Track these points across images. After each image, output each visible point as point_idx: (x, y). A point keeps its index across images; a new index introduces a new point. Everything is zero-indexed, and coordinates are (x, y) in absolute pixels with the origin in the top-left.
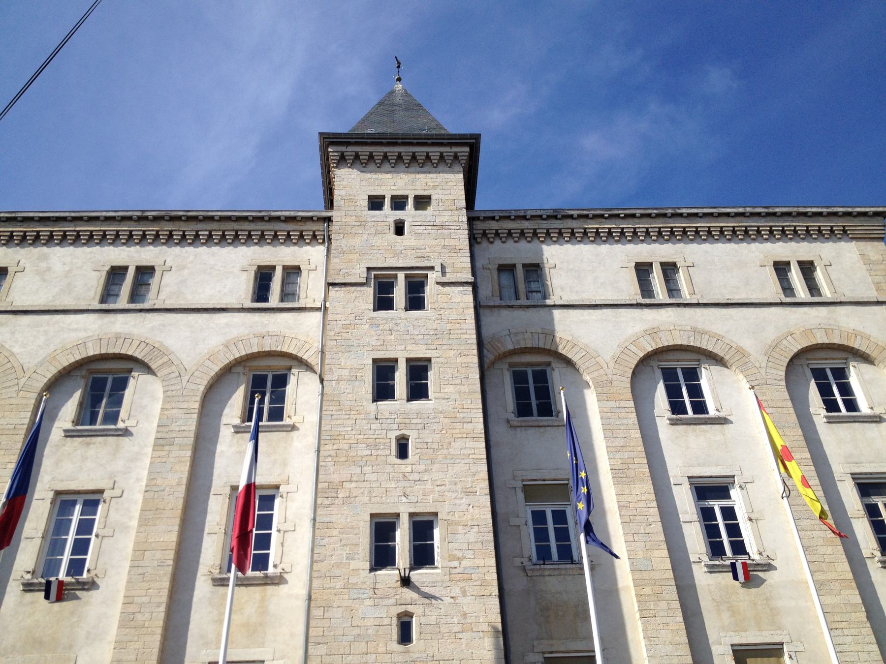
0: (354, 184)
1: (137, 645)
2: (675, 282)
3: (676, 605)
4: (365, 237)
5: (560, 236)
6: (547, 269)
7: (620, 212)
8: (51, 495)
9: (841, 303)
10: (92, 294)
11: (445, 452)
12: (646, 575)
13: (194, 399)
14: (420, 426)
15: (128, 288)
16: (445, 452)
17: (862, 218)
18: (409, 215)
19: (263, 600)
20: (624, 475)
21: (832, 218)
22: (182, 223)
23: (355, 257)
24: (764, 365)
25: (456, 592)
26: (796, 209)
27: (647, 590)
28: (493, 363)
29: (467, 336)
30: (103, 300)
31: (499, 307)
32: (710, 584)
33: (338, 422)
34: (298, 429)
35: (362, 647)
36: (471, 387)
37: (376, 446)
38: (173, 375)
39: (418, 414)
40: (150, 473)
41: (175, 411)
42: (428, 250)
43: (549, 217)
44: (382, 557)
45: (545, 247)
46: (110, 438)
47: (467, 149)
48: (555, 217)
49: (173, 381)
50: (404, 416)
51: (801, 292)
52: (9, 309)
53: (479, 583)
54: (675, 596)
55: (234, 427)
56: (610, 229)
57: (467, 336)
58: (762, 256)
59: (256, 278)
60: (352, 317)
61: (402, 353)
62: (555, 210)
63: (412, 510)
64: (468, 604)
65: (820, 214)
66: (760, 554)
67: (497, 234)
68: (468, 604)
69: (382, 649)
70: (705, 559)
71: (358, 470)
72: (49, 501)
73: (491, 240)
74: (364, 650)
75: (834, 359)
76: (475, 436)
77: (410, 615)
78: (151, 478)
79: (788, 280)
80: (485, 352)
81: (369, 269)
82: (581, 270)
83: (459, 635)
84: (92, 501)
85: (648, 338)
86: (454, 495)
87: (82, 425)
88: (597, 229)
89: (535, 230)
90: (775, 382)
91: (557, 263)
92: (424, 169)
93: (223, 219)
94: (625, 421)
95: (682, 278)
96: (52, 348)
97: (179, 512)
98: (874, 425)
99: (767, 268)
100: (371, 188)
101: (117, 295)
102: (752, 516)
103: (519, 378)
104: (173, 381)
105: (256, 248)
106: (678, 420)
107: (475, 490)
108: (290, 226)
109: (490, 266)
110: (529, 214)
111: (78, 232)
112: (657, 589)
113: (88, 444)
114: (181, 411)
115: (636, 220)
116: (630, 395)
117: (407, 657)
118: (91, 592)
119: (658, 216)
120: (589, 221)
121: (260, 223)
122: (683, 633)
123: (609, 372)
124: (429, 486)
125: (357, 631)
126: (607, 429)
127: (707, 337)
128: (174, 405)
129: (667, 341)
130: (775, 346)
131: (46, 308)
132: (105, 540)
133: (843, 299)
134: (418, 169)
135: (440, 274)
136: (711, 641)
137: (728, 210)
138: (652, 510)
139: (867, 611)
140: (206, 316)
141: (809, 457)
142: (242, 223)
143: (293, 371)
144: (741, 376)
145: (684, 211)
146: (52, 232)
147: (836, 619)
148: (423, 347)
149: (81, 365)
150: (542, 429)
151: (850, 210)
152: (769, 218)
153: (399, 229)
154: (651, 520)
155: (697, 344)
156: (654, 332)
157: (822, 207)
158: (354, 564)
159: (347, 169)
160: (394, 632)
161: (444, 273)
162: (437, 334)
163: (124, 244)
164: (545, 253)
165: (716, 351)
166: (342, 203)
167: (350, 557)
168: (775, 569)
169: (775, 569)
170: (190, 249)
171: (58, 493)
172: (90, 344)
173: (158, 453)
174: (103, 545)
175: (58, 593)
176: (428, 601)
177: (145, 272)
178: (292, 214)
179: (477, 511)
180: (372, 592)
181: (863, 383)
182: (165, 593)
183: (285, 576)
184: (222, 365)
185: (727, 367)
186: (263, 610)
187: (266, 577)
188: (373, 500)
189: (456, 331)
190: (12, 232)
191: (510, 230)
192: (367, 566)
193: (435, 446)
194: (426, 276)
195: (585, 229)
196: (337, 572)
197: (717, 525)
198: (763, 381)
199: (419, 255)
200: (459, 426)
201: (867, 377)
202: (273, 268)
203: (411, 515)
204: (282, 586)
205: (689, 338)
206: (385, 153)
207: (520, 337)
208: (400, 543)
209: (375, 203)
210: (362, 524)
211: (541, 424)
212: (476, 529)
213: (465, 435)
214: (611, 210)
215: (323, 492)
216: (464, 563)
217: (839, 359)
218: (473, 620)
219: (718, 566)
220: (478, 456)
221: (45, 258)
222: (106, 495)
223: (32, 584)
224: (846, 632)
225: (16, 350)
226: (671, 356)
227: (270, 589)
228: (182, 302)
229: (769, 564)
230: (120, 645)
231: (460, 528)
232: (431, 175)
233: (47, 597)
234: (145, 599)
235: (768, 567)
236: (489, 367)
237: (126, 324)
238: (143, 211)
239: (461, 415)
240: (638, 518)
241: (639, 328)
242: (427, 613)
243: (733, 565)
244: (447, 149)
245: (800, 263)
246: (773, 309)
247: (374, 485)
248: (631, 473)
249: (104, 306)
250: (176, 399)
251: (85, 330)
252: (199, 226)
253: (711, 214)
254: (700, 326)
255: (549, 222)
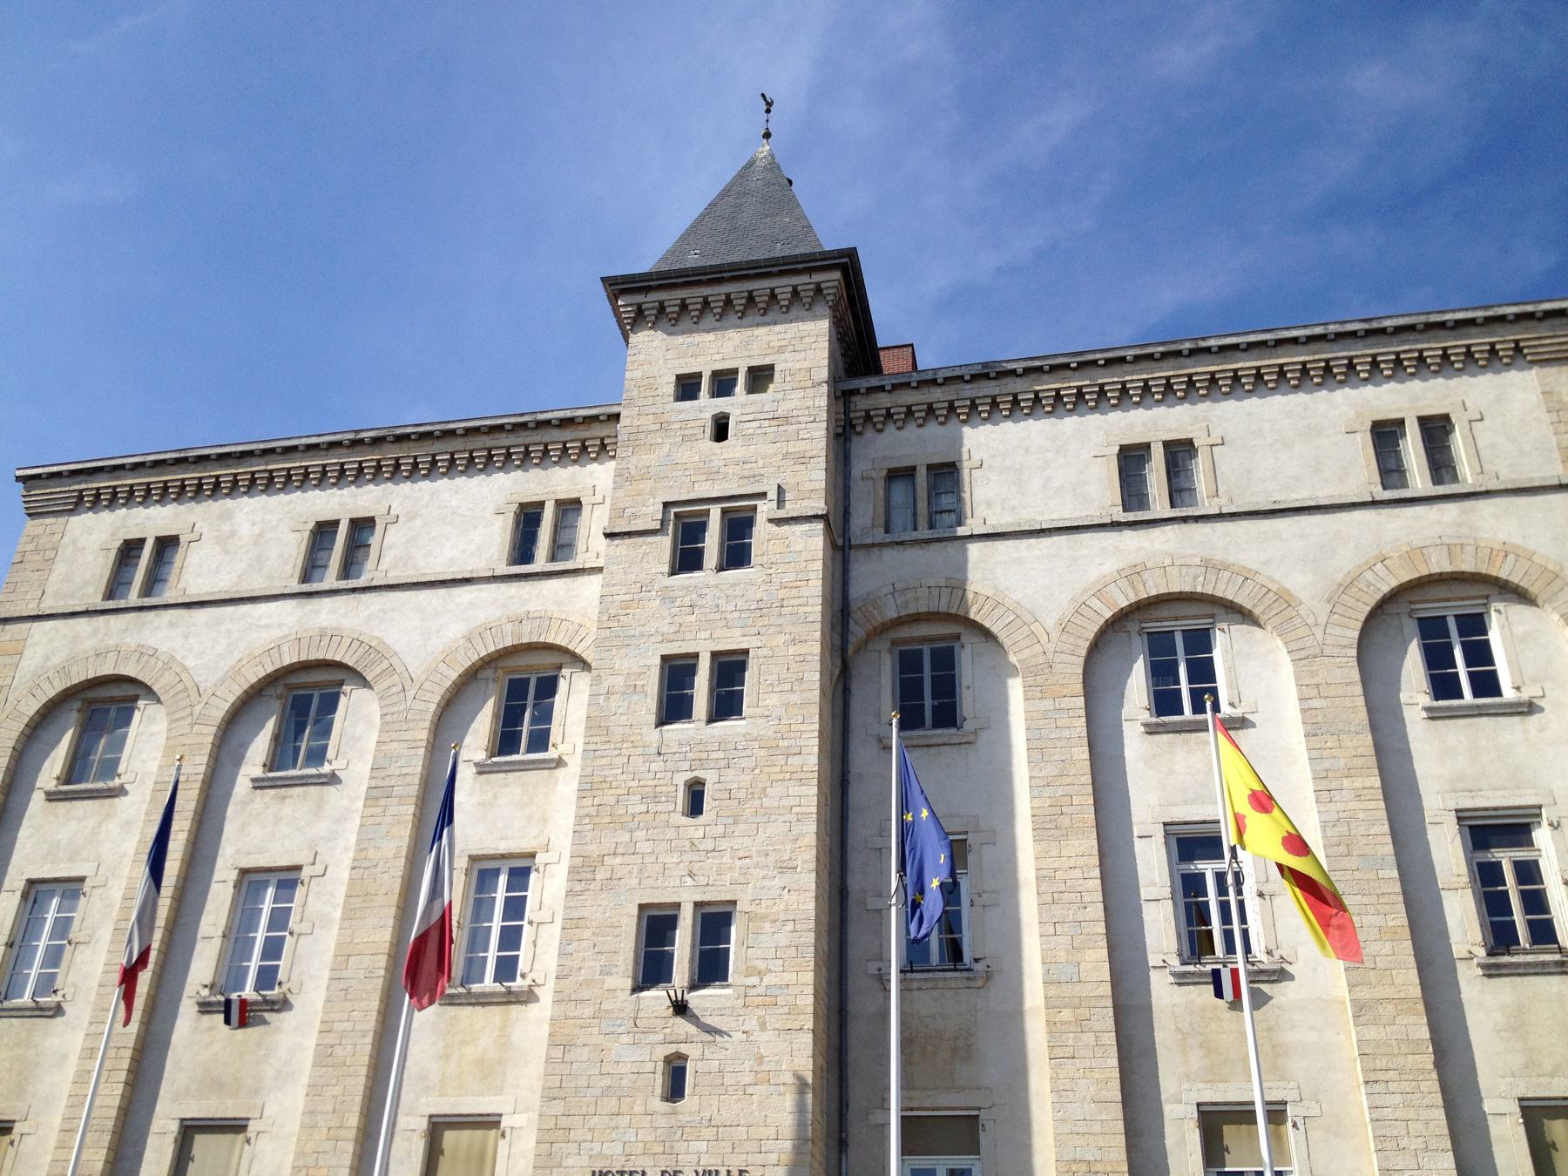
0: (658, 355)
1: (337, 1090)
2: (1189, 474)
3: (1110, 1039)
4: (666, 449)
5: (994, 410)
6: (966, 472)
7: (1098, 356)
8: (234, 875)
9: (1488, 494)
10: (289, 569)
11: (757, 803)
12: (1066, 990)
13: (422, 725)
14: (722, 763)
15: (338, 553)
16: (757, 803)
17: (1557, 322)
18: (738, 404)
19: (504, 1026)
20: (1052, 825)
21: (1497, 327)
22: (411, 444)
23: (647, 485)
24: (1322, 620)
25: (752, 1023)
26: (1423, 319)
27: (1066, 1015)
28: (866, 642)
29: (808, 609)
30: (305, 577)
31: (881, 545)
32: (1173, 1001)
33: (604, 761)
34: (566, 765)
35: (611, 1104)
36: (805, 695)
37: (655, 798)
38: (394, 690)
39: (721, 745)
40: (359, 840)
41: (394, 745)
42: (761, 463)
43: (975, 378)
44: (653, 970)
45: (967, 431)
46: (312, 788)
47: (837, 275)
48: (987, 376)
49: (395, 699)
50: (700, 747)
51: (1419, 478)
52: (180, 601)
53: (786, 1010)
54: (1110, 1023)
55: (477, 765)
56: (1079, 388)
57: (808, 609)
58: (1352, 414)
59: (517, 523)
60: (636, 588)
61: (704, 645)
62: (985, 365)
63: (699, 898)
64: (767, 1042)
65: (1471, 322)
66: (1269, 953)
67: (889, 415)
68: (767, 1042)
69: (638, 1108)
70: (1175, 962)
71: (626, 837)
72: (231, 884)
73: (879, 426)
74: (615, 1110)
75: (1463, 599)
76: (803, 776)
77: (685, 1058)
78: (360, 850)
79: (1398, 455)
80: (852, 626)
81: (666, 505)
82: (1028, 469)
83: (750, 1090)
84: (288, 879)
85: (1123, 583)
86: (763, 873)
87: (278, 769)
88: (1058, 391)
89: (951, 403)
90: (1336, 651)
91: (985, 457)
92: (767, 318)
93: (470, 432)
94: (1066, 733)
95: (1200, 468)
96: (237, 656)
97: (394, 899)
98: (1516, 719)
99: (1358, 435)
100: (681, 361)
101: (325, 567)
102: (1265, 889)
103: (908, 663)
104: (395, 699)
105: (518, 475)
106: (1158, 725)
107: (794, 864)
108: (566, 434)
109: (873, 474)
110: (940, 376)
111: (271, 471)
112: (1084, 1012)
113: (284, 798)
114: (405, 745)
115: (1127, 367)
116: (1080, 686)
117: (673, 1121)
118: (283, 1014)
119: (1165, 355)
120: (1045, 377)
121: (523, 433)
122: (1116, 1084)
123: (1050, 647)
124: (727, 859)
125: (606, 1082)
126: (1036, 749)
127: (1227, 574)
128: (395, 736)
129: (1155, 586)
130: (1348, 586)
131: (228, 596)
132: (302, 938)
133: (1493, 485)
134: (759, 319)
135: (775, 504)
136: (1163, 1097)
137: (1295, 333)
138: (1091, 882)
139: (1435, 1052)
140: (442, 592)
141: (1378, 784)
142: (497, 435)
143: (565, 672)
144: (1280, 643)
145: (1212, 343)
146: (235, 475)
147: (1379, 1065)
148: (738, 632)
149: (276, 679)
150: (933, 751)
151: (1530, 308)
152: (1371, 340)
153: (721, 430)
154: (1087, 899)
155: (1208, 590)
156: (1134, 573)
157: (1475, 309)
158: (611, 982)
159: (647, 332)
160: (658, 1082)
161: (781, 502)
162: (761, 608)
163: (334, 485)
164: (966, 441)
165: (1238, 600)
166: (635, 393)
167: (606, 971)
168: (1292, 978)
169: (1292, 978)
170: (425, 485)
171: (244, 872)
172: (285, 648)
173: (370, 811)
174: (299, 947)
175: (241, 1015)
176: (710, 1038)
177: (362, 526)
178: (568, 414)
179: (794, 897)
180: (631, 1023)
181: (1510, 642)
182: (373, 1016)
183: (537, 990)
184: (461, 670)
185: (1260, 626)
186: (504, 1041)
187: (509, 992)
188: (644, 882)
189: (792, 602)
190: (183, 480)
191: (909, 408)
192: (628, 983)
193: (742, 794)
194: (755, 508)
195: (1036, 393)
196: (586, 994)
197: (1207, 903)
198: (1317, 650)
199: (746, 473)
200: (781, 760)
201: (1518, 630)
202: (541, 504)
203: (697, 905)
204: (531, 1006)
205: (1196, 577)
206: (706, 298)
207: (910, 595)
208: (680, 947)
209: (687, 387)
210: (625, 920)
211: (932, 741)
212: (790, 926)
213: (788, 776)
214: (1081, 353)
215: (583, 870)
216: (769, 979)
217: (1475, 598)
218: (772, 1066)
219: (1193, 974)
220: (804, 810)
221: (227, 516)
222: (305, 874)
223: (209, 1004)
224: (1392, 1087)
225: (189, 663)
226: (1165, 612)
227: (515, 1009)
228: (412, 572)
229: (1282, 971)
230: (314, 1090)
231: (767, 925)
232: (778, 328)
233: (227, 1021)
234: (348, 1026)
235: (1280, 975)
236: (858, 650)
237: (334, 612)
238: (357, 432)
239: (786, 743)
240: (1065, 896)
241: (1110, 566)
242: (708, 1055)
243: (1216, 975)
244: (804, 279)
245: (1423, 421)
246: (1357, 514)
247: (647, 860)
248: (1065, 821)
249: (306, 588)
250: (397, 727)
251: (279, 626)
252: (437, 447)
253: (1264, 343)
254: (1218, 556)
255: (975, 385)
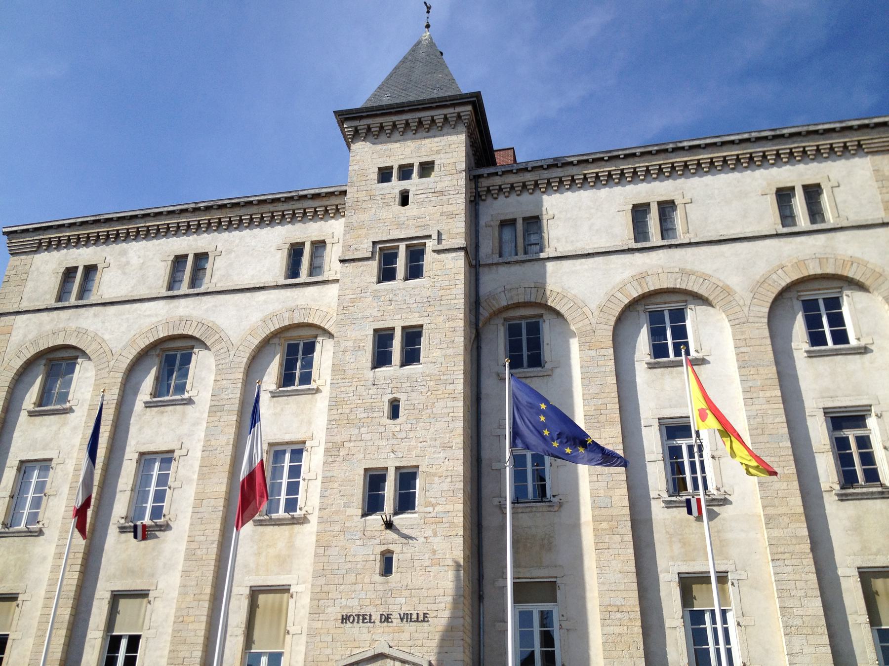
0: (368, 156)
1: (198, 574)
3: (629, 538)
4: (374, 211)
5: (561, 185)
6: (545, 222)
7: (620, 153)
8: (136, 456)
9: (842, 229)
10: (160, 282)
11: (429, 411)
12: (604, 512)
14: (409, 389)
15: (187, 273)
16: (429, 411)
17: (882, 129)
18: (414, 184)
21: (847, 133)
22: (227, 210)
23: (363, 232)
24: (748, 302)
25: (429, 533)
26: (805, 129)
27: (604, 525)
29: (456, 301)
30: (170, 287)
31: (497, 264)
32: (664, 517)
34: (321, 391)
35: (351, 578)
36: (456, 350)
38: (223, 351)
40: (206, 436)
41: (225, 382)
43: (550, 167)
44: (373, 504)
45: (545, 197)
47: (469, 108)
48: (556, 166)
51: (803, 221)
53: (448, 525)
56: (609, 172)
57: (456, 301)
58: (765, 183)
59: (289, 255)
61: (397, 323)
62: (555, 159)
63: (398, 465)
64: (438, 543)
65: (833, 130)
66: (718, 489)
67: (500, 189)
68: (438, 543)
69: (367, 580)
70: (665, 495)
71: (357, 431)
73: (495, 196)
74: (354, 581)
77: (392, 552)
78: (207, 440)
79: (791, 207)
80: (481, 310)
81: (374, 243)
82: (581, 219)
83: (428, 569)
84: (167, 458)
85: (635, 283)
88: (597, 173)
89: (536, 182)
90: (757, 320)
91: (556, 213)
92: (430, 134)
93: (261, 202)
94: (603, 369)
95: (678, 218)
96: (133, 333)
98: (858, 356)
99: (768, 197)
100: (382, 160)
102: (715, 454)
103: (513, 331)
106: (655, 363)
109: (492, 223)
110: (530, 166)
111: (148, 227)
113: (162, 412)
114: (229, 381)
115: (637, 159)
116: (611, 342)
117: (386, 587)
118: (167, 533)
119: (658, 152)
120: (589, 166)
121: (291, 203)
122: (632, 563)
123: (593, 321)
124: (413, 443)
125: (349, 566)
127: (694, 277)
128: (224, 377)
132: (176, 490)
135: (436, 242)
136: (659, 570)
140: (248, 294)
141: (779, 393)
143: (319, 339)
144: (724, 316)
145: (685, 144)
146: (128, 229)
147: (779, 550)
148: (417, 315)
149: (156, 346)
151: (866, 122)
153: (404, 200)
155: (683, 287)
156: (642, 277)
158: (349, 511)
160: (378, 566)
161: (440, 240)
162: (429, 301)
165: (700, 292)
166: (355, 178)
168: (731, 503)
169: (731, 503)
170: (236, 233)
171: (142, 454)
172: (160, 328)
175: (143, 533)
177: (201, 258)
178: (317, 191)
180: (362, 533)
181: (854, 312)
182: (217, 532)
183: (308, 516)
184: (260, 339)
186: (291, 545)
187: (293, 518)
188: (367, 456)
189: (447, 297)
190: (98, 233)
191: (512, 185)
192: (360, 512)
194: (425, 244)
195: (585, 175)
197: (683, 462)
198: (745, 320)
199: (420, 224)
200: (442, 387)
201: (859, 306)
202: (303, 244)
204: (305, 525)
205: (676, 280)
207: (514, 292)
208: (388, 492)
209: (385, 175)
210: (357, 477)
212: (449, 479)
213: (446, 396)
214: (610, 151)
215: (332, 450)
216: (438, 509)
217: (835, 288)
218: (440, 556)
220: (456, 414)
221: (124, 253)
222: (176, 454)
224: (787, 562)
225: (106, 337)
226: (659, 299)
227: (297, 527)
228: (230, 284)
229: (725, 499)
230: (185, 574)
231: (437, 478)
232: (436, 139)
233: (135, 537)
235: (724, 502)
236: (485, 324)
239: (445, 377)
241: (627, 274)
242: (405, 550)
243: (688, 502)
244: (451, 110)
245: (806, 188)
246: (768, 242)
249: (170, 293)
251: (156, 315)
252: (242, 211)
253: (715, 144)
254: (689, 267)
255: (550, 171)
